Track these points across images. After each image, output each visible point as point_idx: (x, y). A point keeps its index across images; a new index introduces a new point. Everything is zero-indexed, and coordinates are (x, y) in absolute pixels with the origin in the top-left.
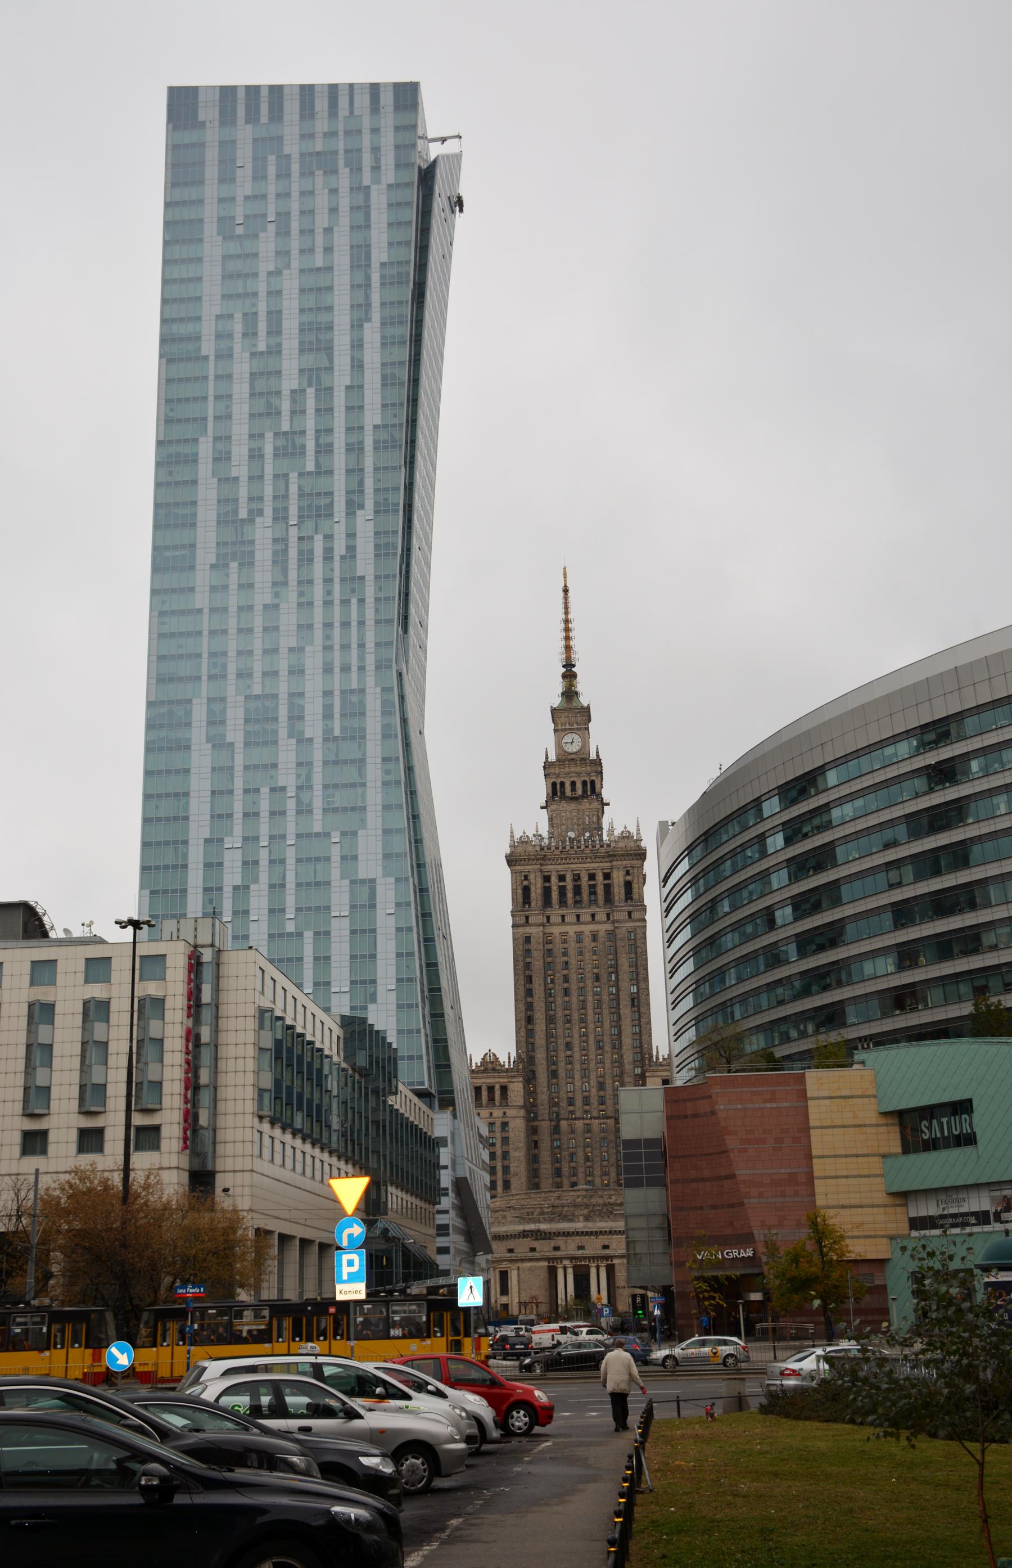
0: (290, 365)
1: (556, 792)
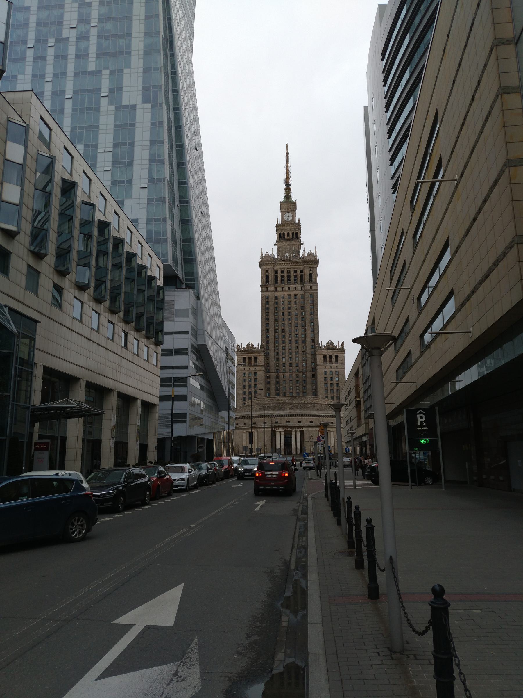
1: (281, 237)
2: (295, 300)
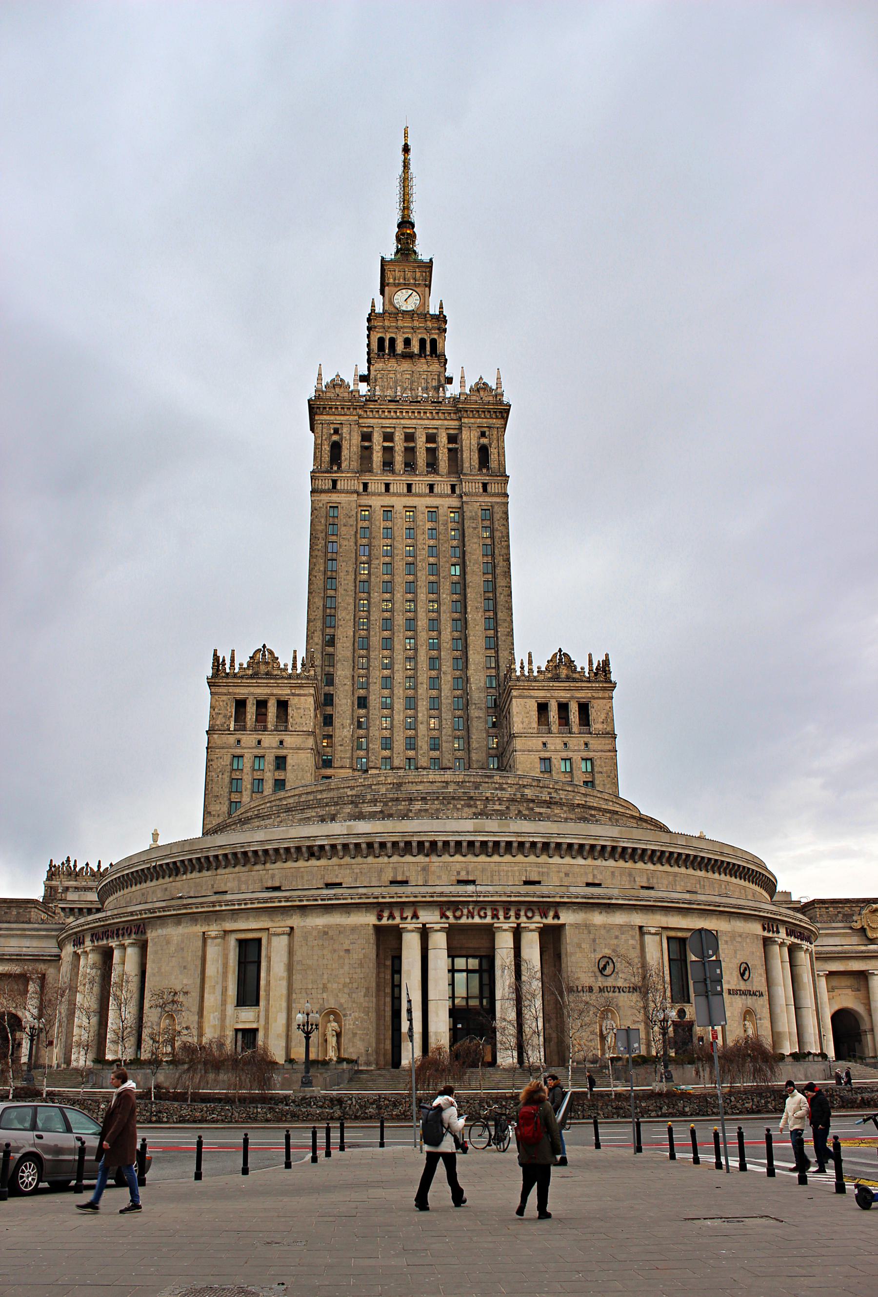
1: (381, 349)
2: (429, 525)
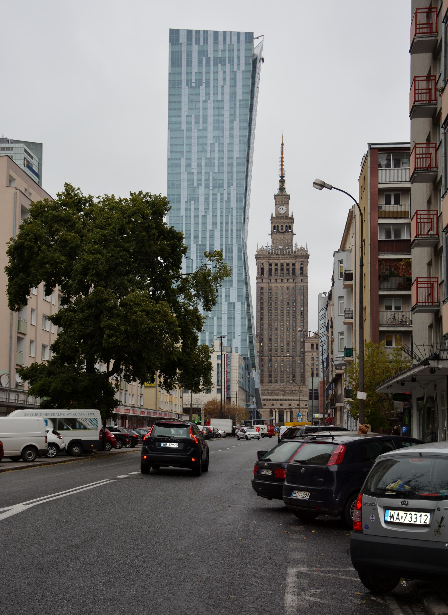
0: (210, 134)
